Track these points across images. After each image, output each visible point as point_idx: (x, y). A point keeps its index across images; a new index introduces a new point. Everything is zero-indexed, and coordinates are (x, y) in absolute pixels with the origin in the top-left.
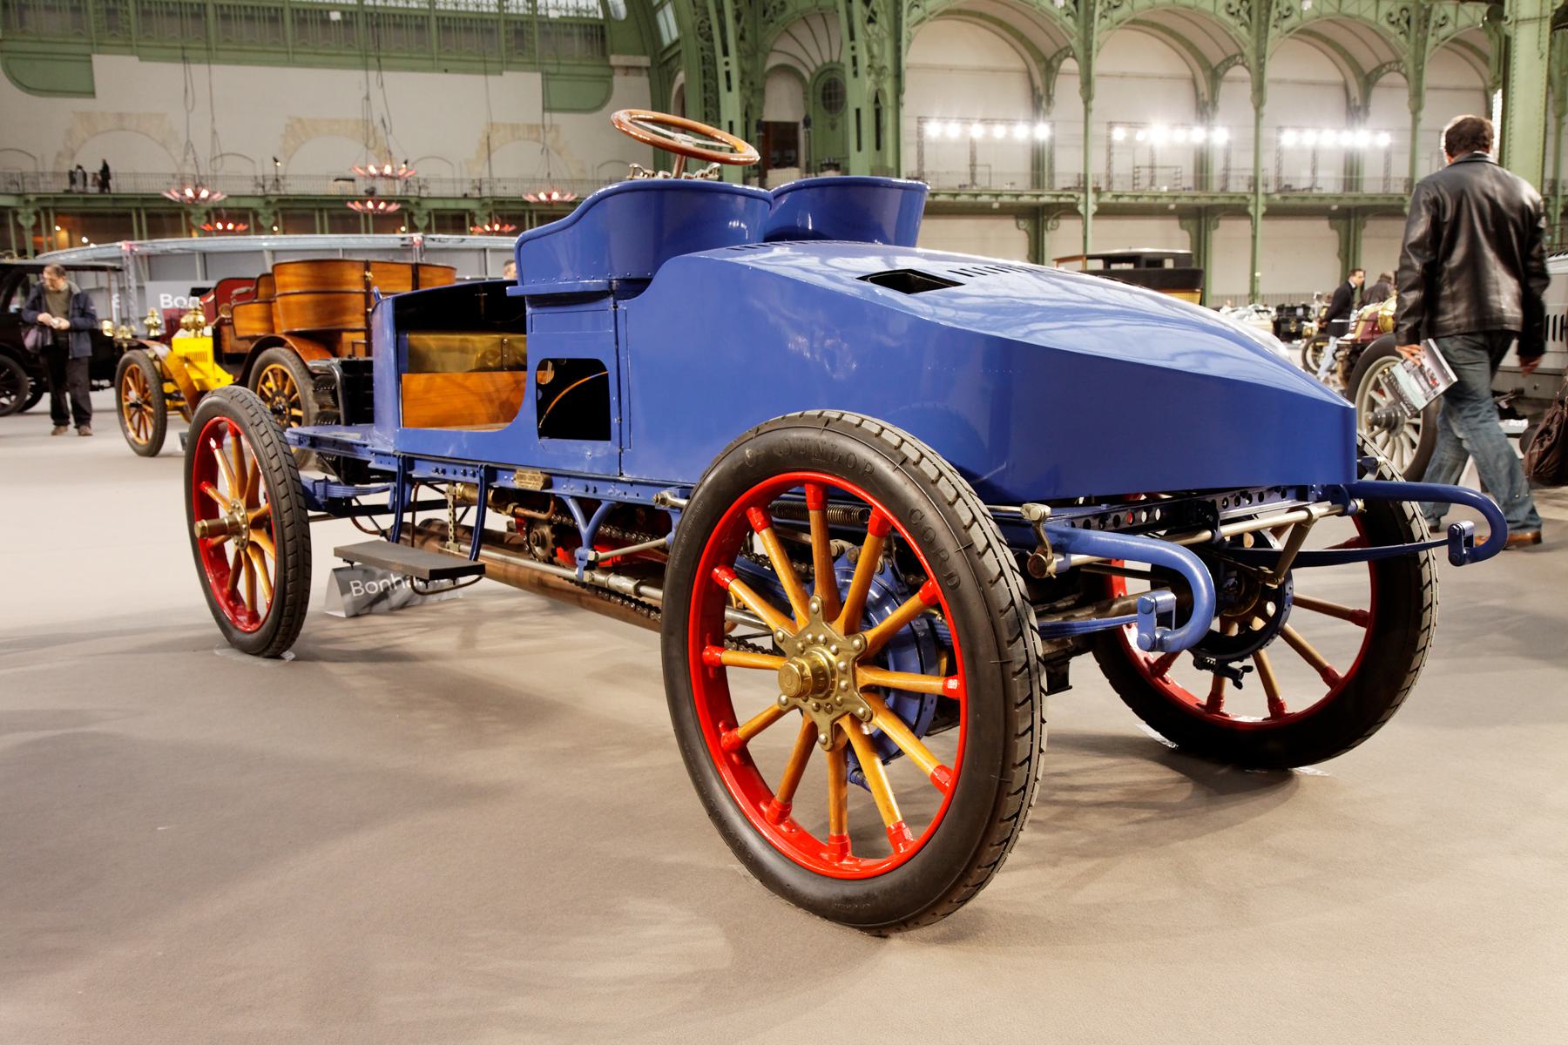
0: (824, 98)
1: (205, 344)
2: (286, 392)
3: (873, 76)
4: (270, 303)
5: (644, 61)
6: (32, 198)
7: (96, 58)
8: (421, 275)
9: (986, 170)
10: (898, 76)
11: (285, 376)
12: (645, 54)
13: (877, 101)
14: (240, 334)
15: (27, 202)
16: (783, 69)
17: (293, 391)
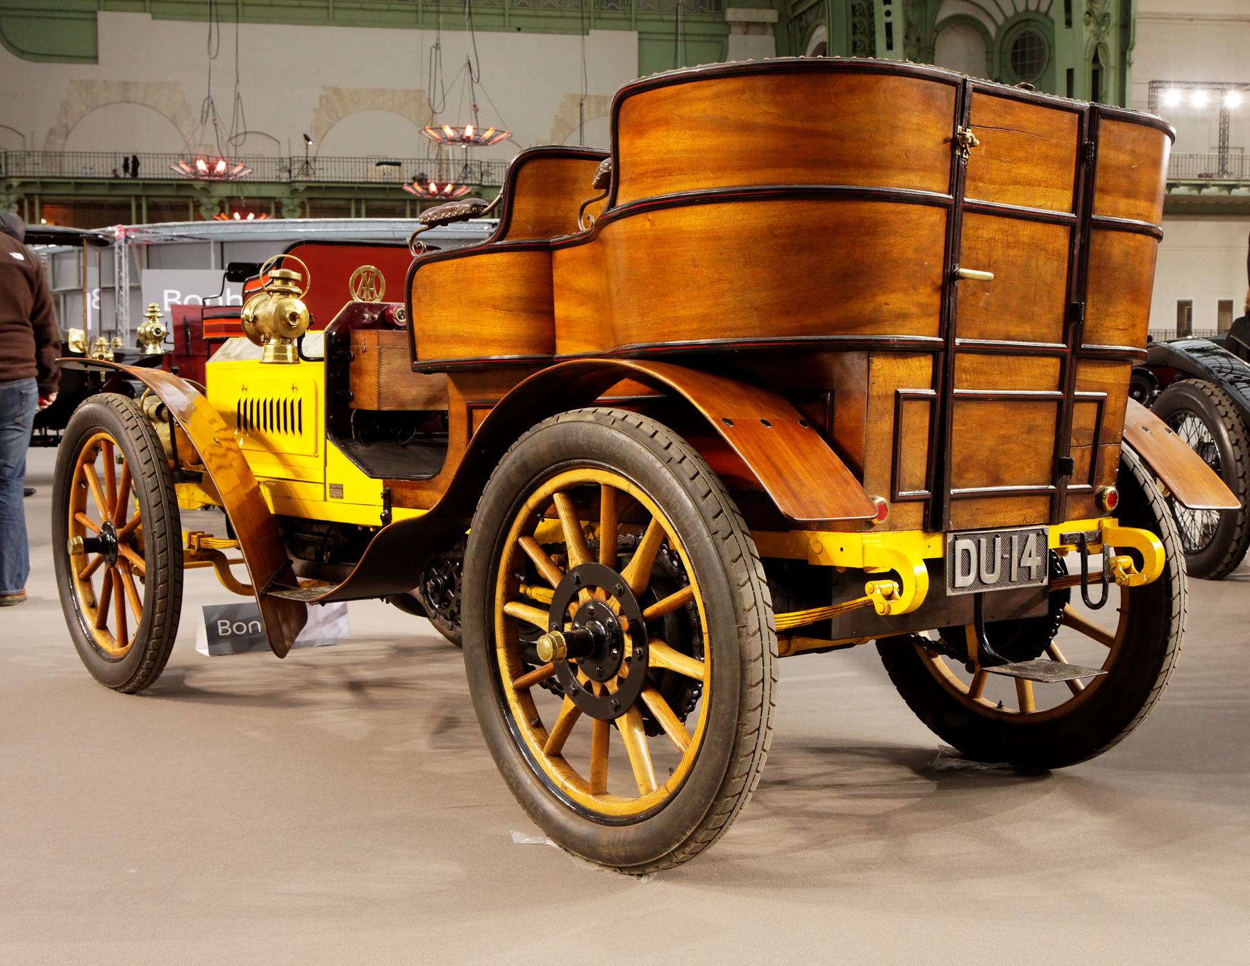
0: (1014, 58)
1: (306, 383)
2: (630, 574)
3: (1092, 27)
4: (548, 250)
5: (770, 16)
6: (15, 182)
7: (102, 16)
8: (1106, 154)
9: (1239, 152)
10: (1126, 26)
11: (633, 516)
12: (772, 8)
13: (1096, 60)
14: (428, 353)
15: (10, 187)
16: (961, 22)
17: (664, 576)
